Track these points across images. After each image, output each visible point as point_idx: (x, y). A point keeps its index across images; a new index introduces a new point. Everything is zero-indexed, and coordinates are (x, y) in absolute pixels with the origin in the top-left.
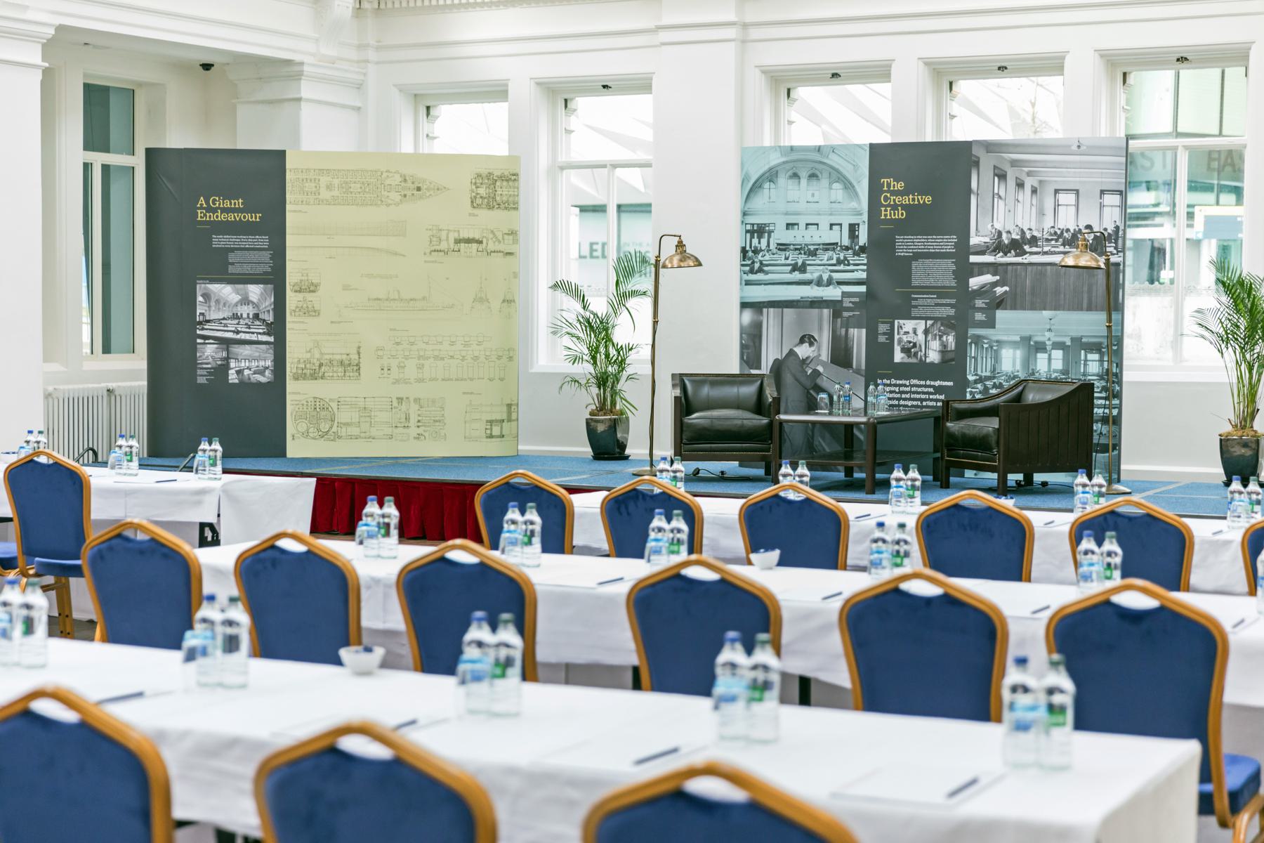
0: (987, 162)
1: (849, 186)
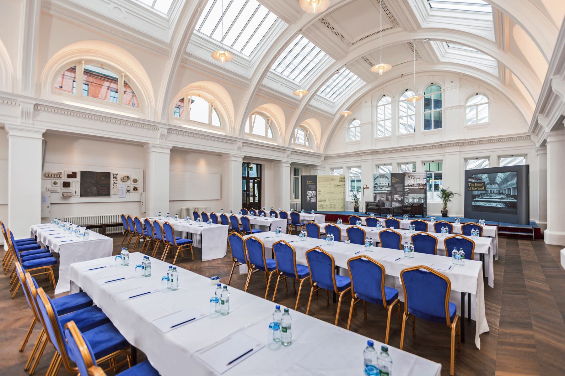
0: (407, 175)
1: (388, 178)
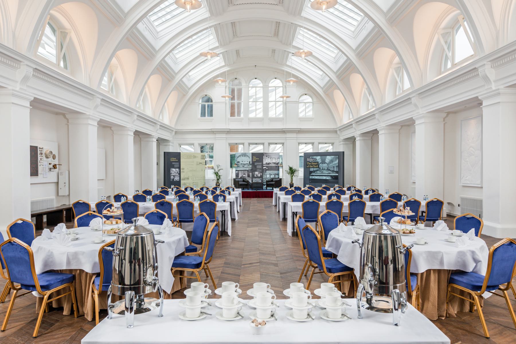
0: (265, 155)
1: (249, 157)
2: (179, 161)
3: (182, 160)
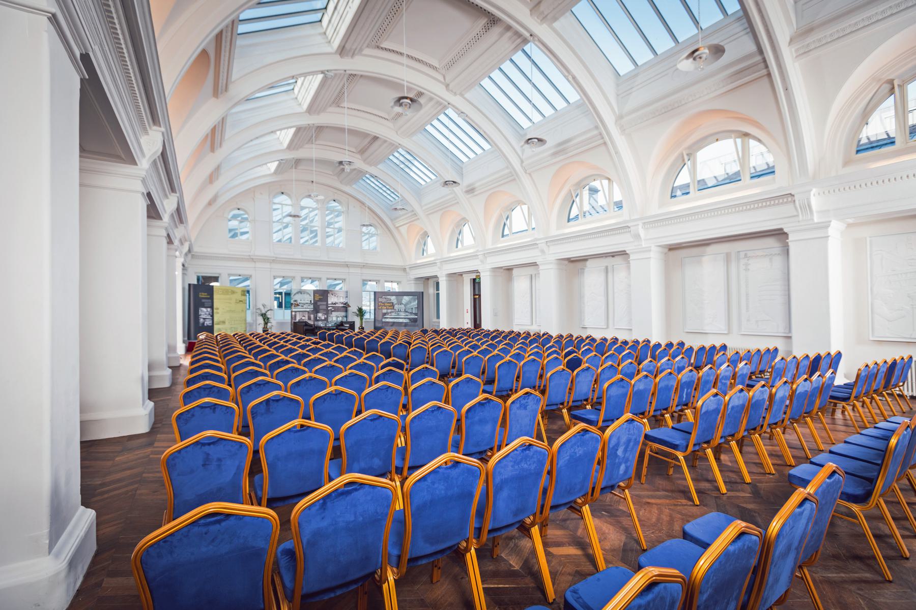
2: (212, 298)
3: (216, 297)
